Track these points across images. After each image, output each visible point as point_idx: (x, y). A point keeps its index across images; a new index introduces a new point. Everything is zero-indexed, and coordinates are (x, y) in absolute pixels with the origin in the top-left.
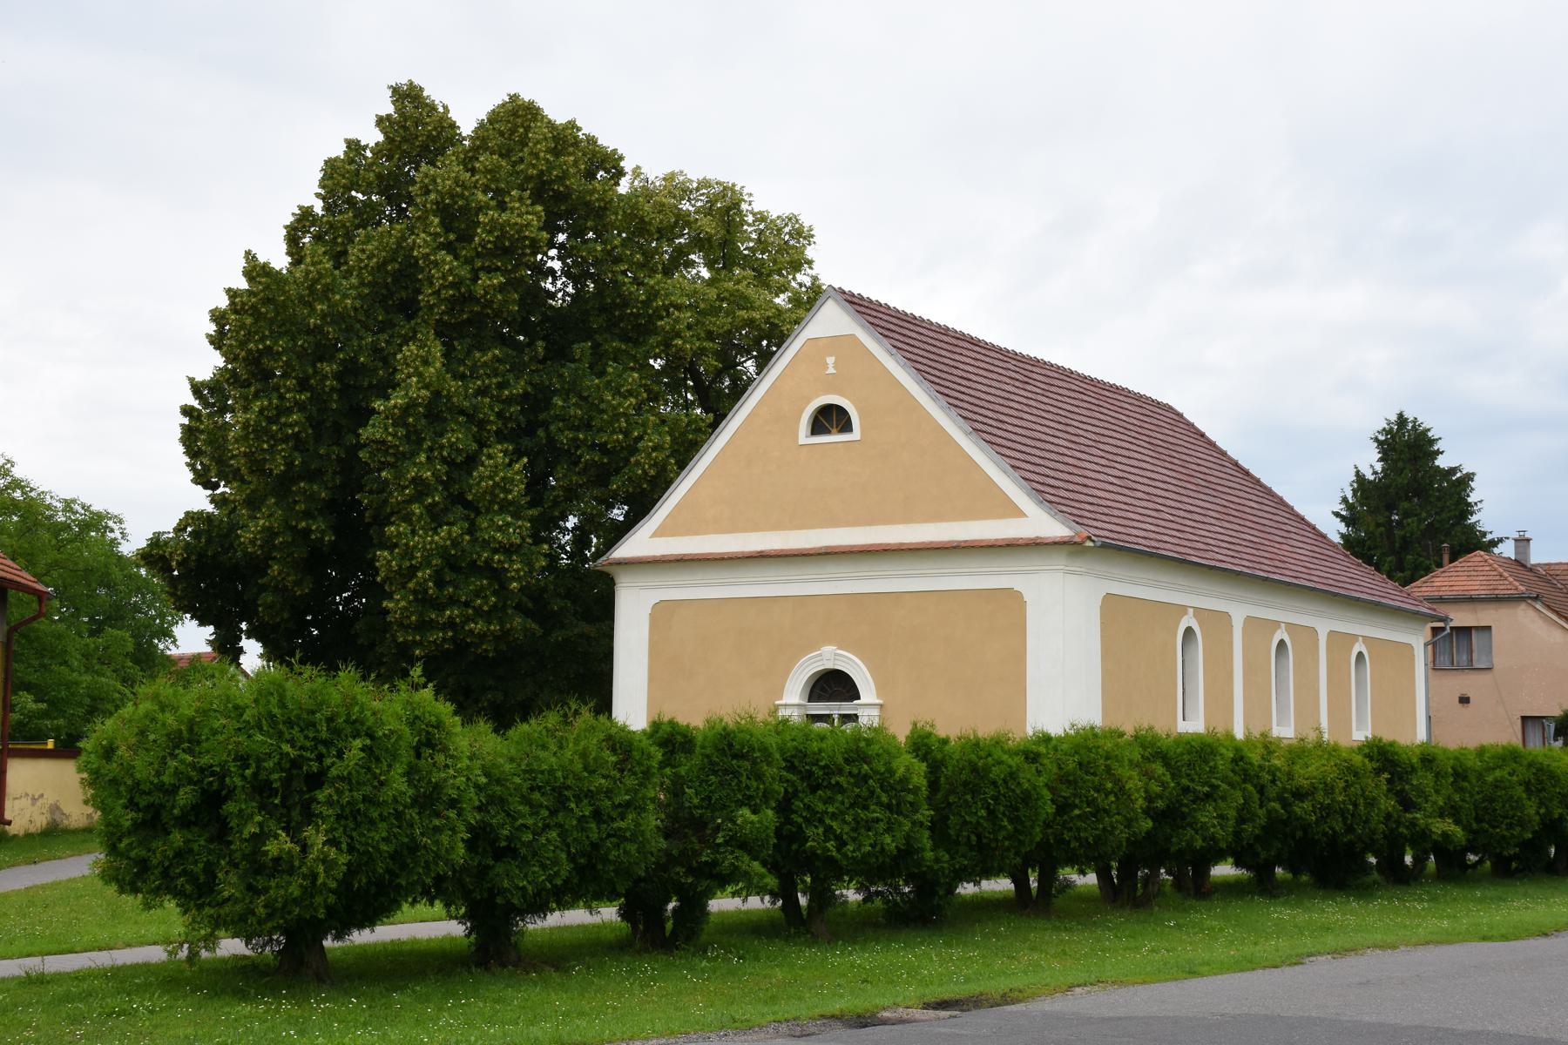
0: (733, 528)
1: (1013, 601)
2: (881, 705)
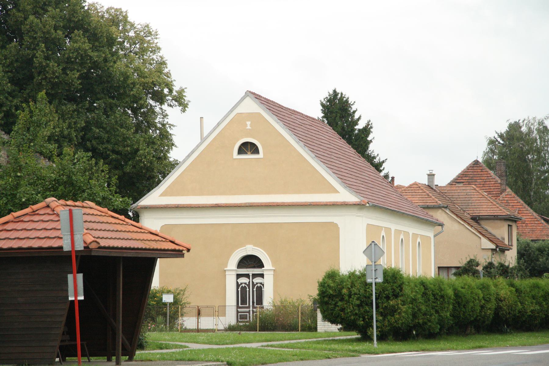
0: (201, 193)
1: (333, 228)
2: (274, 270)
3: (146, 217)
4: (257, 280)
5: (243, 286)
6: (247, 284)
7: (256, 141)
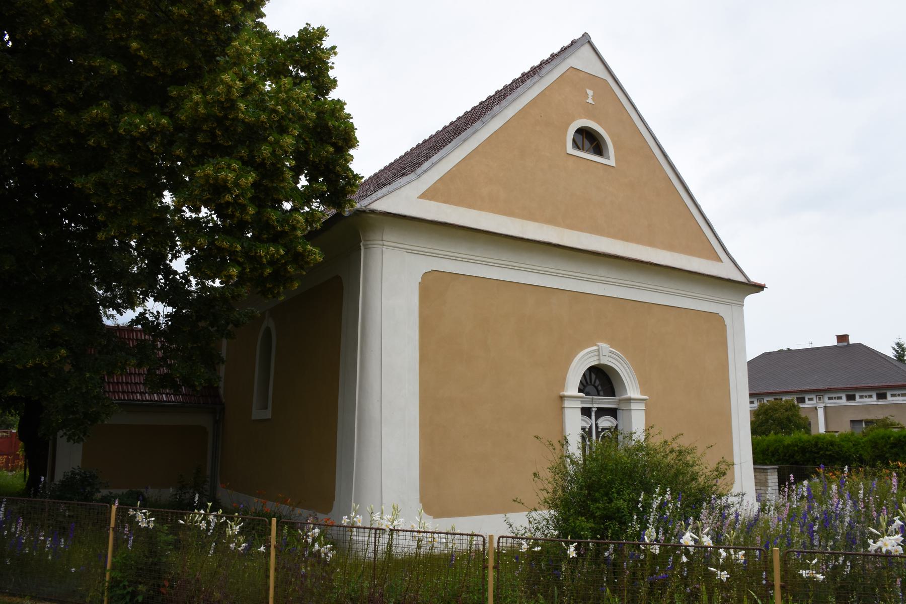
3: (385, 243)
4: (606, 422)
7: (603, 130)
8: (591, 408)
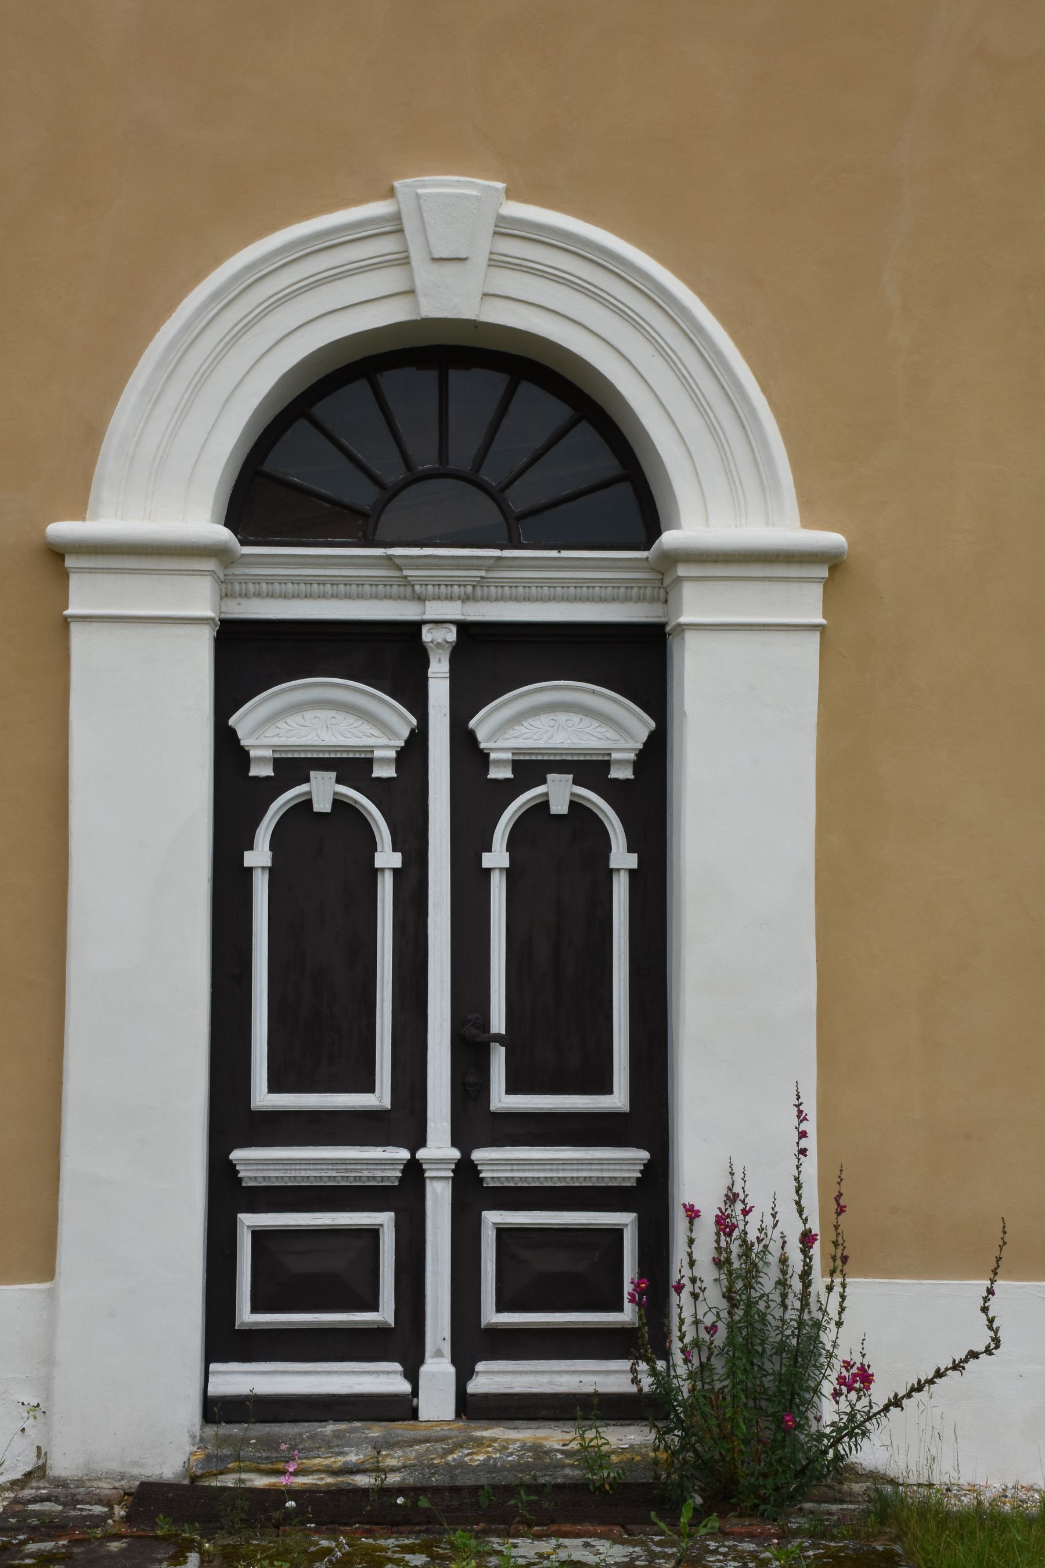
5: (322, 805)
6: (384, 772)
8: (414, 628)
